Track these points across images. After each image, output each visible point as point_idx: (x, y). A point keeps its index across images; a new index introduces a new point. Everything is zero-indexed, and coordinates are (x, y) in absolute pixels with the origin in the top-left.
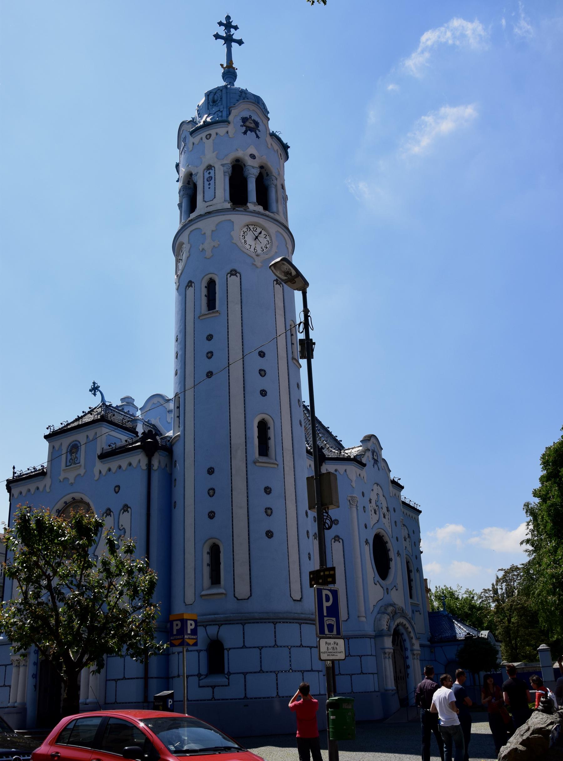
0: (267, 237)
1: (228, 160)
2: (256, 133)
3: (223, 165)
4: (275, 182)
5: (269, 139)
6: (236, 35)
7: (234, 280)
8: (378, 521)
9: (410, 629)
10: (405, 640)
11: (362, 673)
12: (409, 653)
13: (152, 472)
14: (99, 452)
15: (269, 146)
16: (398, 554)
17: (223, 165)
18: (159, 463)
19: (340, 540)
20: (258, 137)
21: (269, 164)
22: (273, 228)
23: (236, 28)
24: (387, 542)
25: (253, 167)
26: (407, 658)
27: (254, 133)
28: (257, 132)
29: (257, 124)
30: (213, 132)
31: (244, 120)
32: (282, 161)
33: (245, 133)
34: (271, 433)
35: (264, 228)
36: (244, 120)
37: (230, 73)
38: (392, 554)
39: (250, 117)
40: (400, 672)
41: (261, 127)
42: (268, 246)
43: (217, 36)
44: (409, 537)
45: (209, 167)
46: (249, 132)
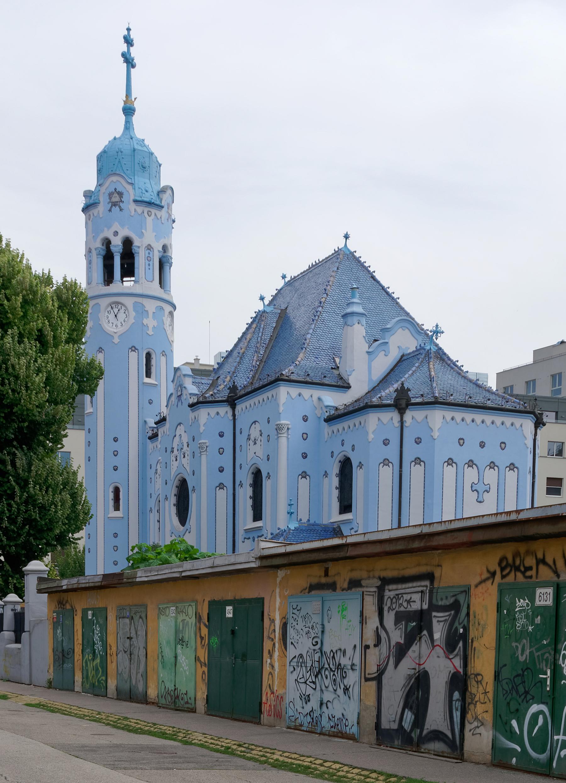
20: (121, 210)
25: (115, 246)
27: (117, 207)
28: (121, 204)
32: (150, 220)
33: (110, 210)
36: (111, 195)
39: (115, 189)
42: (126, 319)
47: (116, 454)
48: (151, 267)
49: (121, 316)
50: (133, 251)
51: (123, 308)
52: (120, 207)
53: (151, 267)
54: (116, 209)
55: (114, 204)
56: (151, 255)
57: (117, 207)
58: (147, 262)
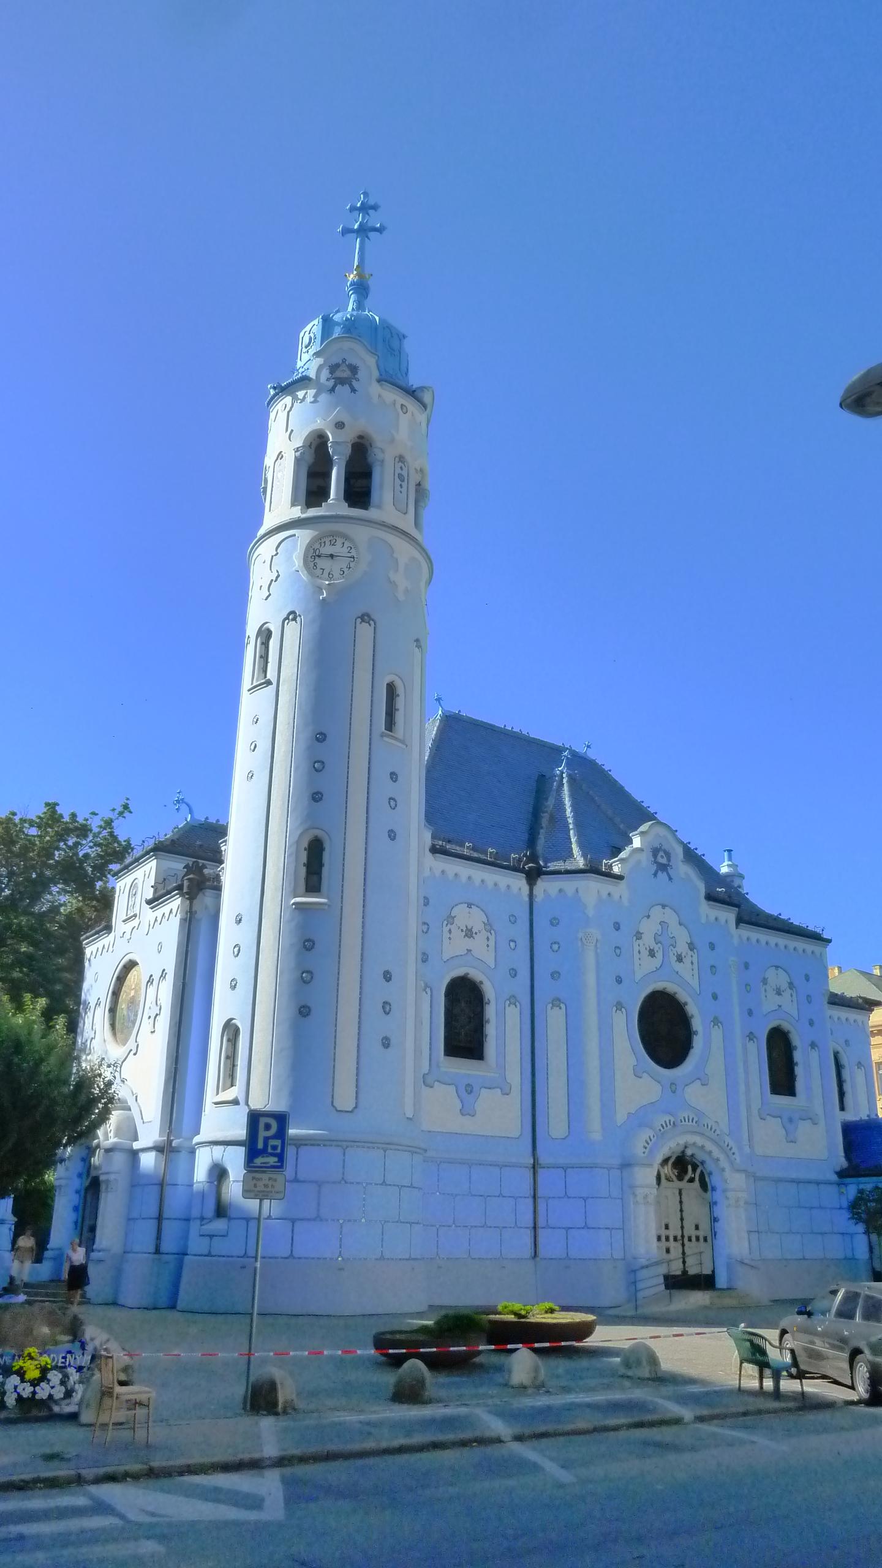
0: (353, 551)
1: (299, 442)
2: (351, 386)
3: (297, 450)
4: (380, 456)
7: (292, 629)
8: (657, 969)
10: (710, 1174)
11: (586, 1227)
14: (150, 894)
19: (562, 1006)
20: (353, 390)
24: (686, 1004)
26: (715, 1203)
27: (347, 387)
28: (354, 383)
29: (354, 369)
35: (346, 537)
38: (697, 1024)
39: (344, 361)
40: (697, 1227)
41: (361, 374)
46: (339, 387)
48: (404, 490)
50: (370, 459)
51: (347, 544)
52: (351, 386)
53: (404, 490)
55: (341, 381)
56: (404, 473)
57: (347, 387)
58: (398, 482)
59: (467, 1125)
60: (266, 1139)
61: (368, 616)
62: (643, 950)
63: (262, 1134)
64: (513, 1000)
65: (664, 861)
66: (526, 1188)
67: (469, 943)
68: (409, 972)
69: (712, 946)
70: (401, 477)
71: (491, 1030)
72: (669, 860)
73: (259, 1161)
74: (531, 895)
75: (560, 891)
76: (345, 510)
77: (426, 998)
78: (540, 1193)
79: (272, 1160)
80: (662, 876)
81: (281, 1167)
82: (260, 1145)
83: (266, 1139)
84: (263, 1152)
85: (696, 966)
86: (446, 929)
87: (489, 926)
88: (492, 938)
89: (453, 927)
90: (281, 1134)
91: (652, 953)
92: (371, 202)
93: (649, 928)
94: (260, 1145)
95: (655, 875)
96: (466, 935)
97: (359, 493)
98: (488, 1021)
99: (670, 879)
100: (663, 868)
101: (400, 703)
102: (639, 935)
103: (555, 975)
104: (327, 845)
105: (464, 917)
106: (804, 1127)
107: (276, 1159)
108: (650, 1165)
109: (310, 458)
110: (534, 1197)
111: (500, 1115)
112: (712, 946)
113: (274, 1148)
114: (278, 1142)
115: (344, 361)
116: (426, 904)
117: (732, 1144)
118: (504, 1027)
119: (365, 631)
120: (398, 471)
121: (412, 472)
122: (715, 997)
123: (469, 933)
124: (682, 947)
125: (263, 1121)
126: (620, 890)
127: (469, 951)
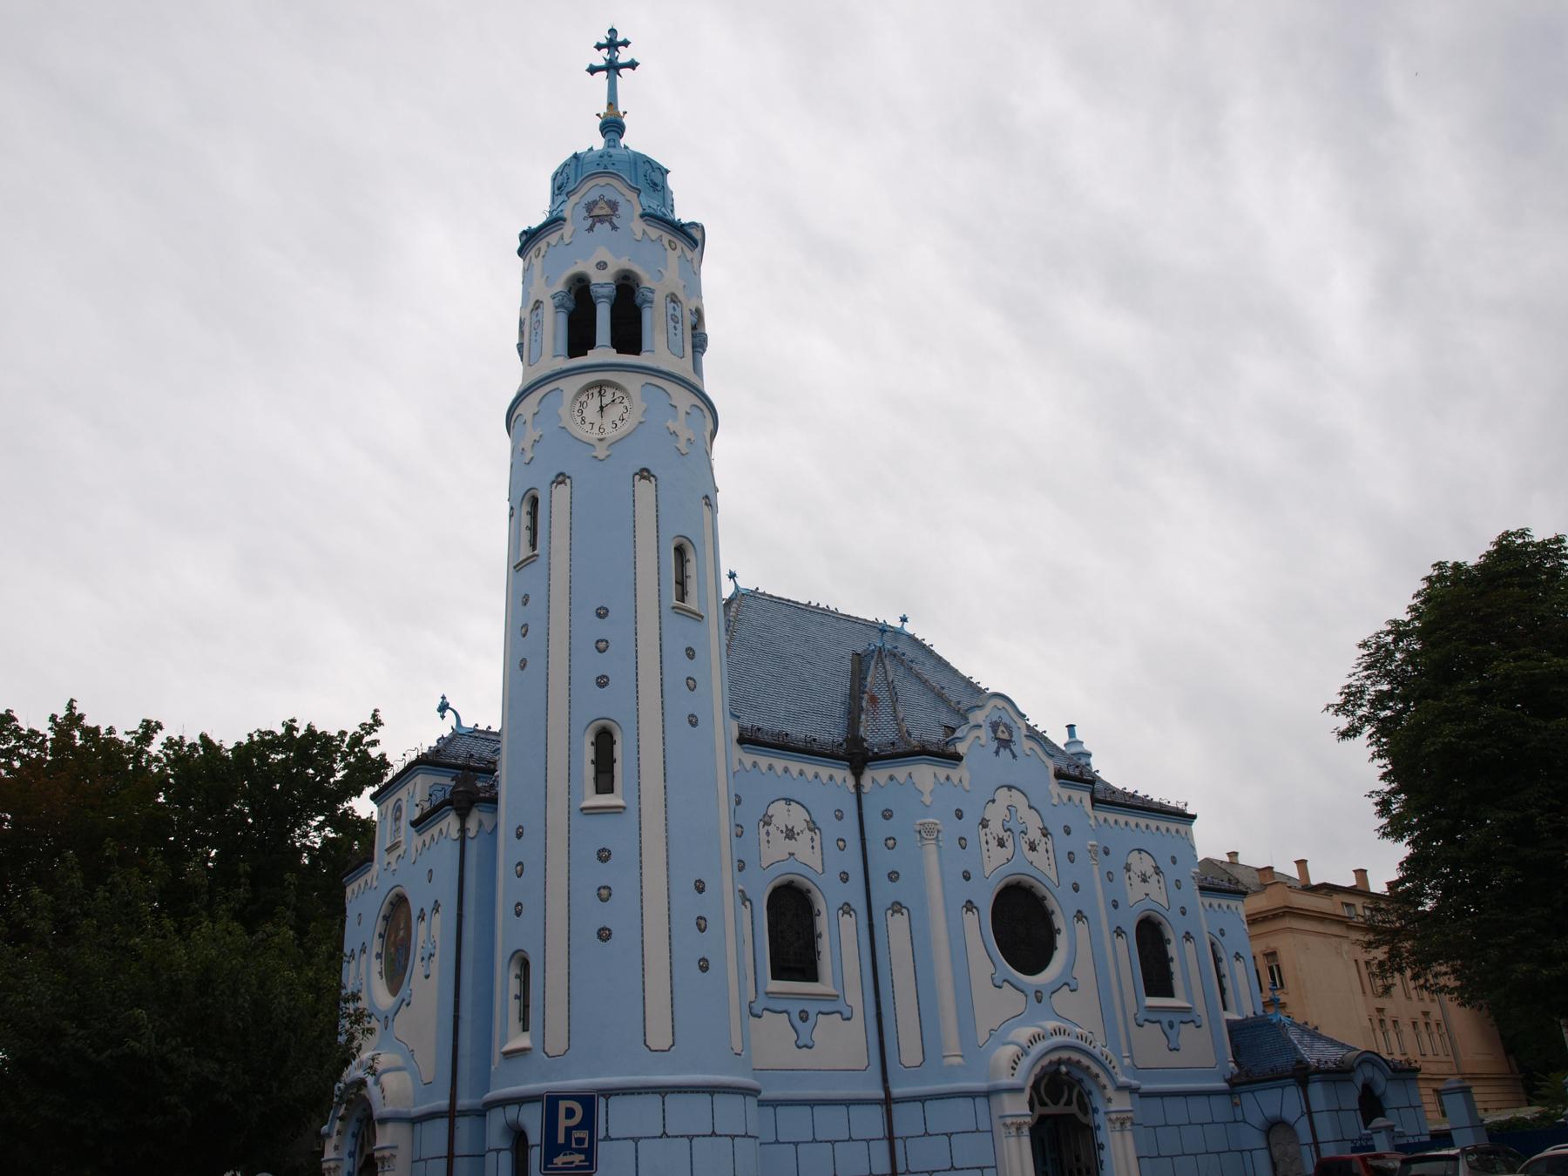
1: (559, 286)
2: (611, 223)
3: (553, 298)
5: (639, 226)
6: (624, 56)
7: (562, 492)
9: (1095, 1069)
10: (1090, 1093)
12: (1100, 1119)
13: (468, 842)
15: (639, 236)
16: (1080, 916)
17: (553, 298)
18: (481, 824)
20: (614, 228)
21: (637, 269)
22: (633, 382)
23: (626, 43)
25: (602, 286)
27: (607, 225)
28: (615, 220)
29: (613, 206)
30: (542, 245)
31: (590, 207)
32: (673, 256)
33: (591, 229)
34: (618, 751)
36: (590, 207)
37: (612, 126)
38: (1059, 921)
39: (602, 197)
41: (621, 211)
43: (593, 70)
44: (1157, 870)
45: (538, 304)
47: (602, 646)
48: (679, 332)
49: (614, 412)
50: (638, 301)
52: (611, 223)
53: (679, 332)
54: (603, 229)
55: (600, 219)
56: (678, 313)
57: (607, 225)
58: (671, 324)
59: (804, 1059)
60: (569, 1130)
61: (647, 470)
62: (990, 838)
63: (563, 1123)
64: (847, 909)
65: (1006, 736)
66: (879, 1130)
67: (791, 845)
68: (725, 883)
69: (1068, 831)
70: (674, 319)
71: (824, 945)
72: (1011, 735)
73: (559, 1161)
74: (858, 786)
75: (891, 778)
76: (612, 356)
77: (746, 913)
78: (897, 1133)
79: (578, 1159)
80: (1005, 753)
81: (591, 1167)
82: (561, 1139)
83: (569, 1130)
84: (566, 1148)
85: (1051, 854)
86: (763, 831)
87: (813, 826)
88: (817, 838)
89: (771, 828)
90: (589, 1122)
91: (1001, 844)
92: (620, 39)
93: (996, 815)
94: (561, 1139)
95: (997, 753)
96: (787, 837)
97: (628, 338)
98: (820, 936)
99: (1014, 756)
100: (1005, 744)
101: (691, 569)
102: (984, 824)
103: (893, 876)
104: (618, 737)
105: (785, 815)
106: (1187, 1031)
107: (582, 1157)
108: (1020, 1090)
109: (571, 305)
110: (891, 1138)
111: (841, 1045)
112: (1068, 831)
113: (580, 1141)
114: (584, 1134)
115: (602, 197)
116: (738, 803)
117: (1111, 1056)
118: (839, 940)
119: (645, 488)
120: (671, 311)
121: (687, 313)
122: (1076, 888)
123: (790, 834)
124: (1034, 834)
125: (563, 1105)
126: (960, 773)
127: (792, 854)
